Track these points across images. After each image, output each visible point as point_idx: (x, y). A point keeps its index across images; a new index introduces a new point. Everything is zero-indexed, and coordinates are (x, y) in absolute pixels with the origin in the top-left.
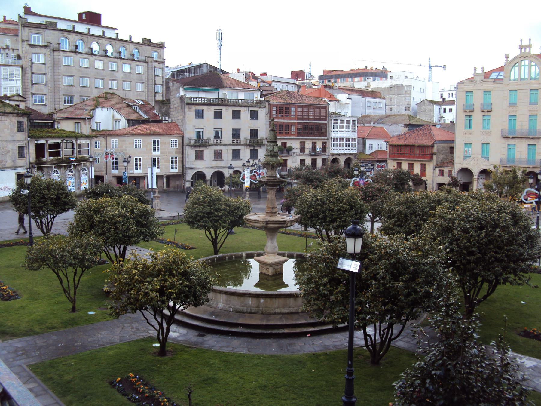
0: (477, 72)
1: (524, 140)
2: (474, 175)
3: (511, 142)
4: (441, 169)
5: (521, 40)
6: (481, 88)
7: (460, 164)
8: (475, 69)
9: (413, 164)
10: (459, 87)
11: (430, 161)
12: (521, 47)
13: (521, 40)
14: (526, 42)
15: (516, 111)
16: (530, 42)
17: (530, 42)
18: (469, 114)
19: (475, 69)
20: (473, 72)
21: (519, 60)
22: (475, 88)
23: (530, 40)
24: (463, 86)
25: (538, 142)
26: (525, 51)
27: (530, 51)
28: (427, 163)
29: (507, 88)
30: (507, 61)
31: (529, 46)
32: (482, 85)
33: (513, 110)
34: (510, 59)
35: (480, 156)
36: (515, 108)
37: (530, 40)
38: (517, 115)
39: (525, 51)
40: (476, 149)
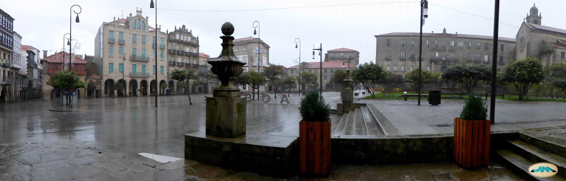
1: (140, 62)
3: (134, 63)
4: (91, 80)
5: (137, 8)
7: (107, 77)
8: (114, 18)
12: (137, 11)
13: (137, 8)
14: (139, 9)
15: (136, 46)
19: (114, 18)
22: (115, 30)
23: (141, 9)
24: (107, 27)
25: (146, 64)
29: (132, 32)
31: (141, 12)
35: (118, 71)
37: (141, 9)
38: (137, 48)
40: (116, 67)
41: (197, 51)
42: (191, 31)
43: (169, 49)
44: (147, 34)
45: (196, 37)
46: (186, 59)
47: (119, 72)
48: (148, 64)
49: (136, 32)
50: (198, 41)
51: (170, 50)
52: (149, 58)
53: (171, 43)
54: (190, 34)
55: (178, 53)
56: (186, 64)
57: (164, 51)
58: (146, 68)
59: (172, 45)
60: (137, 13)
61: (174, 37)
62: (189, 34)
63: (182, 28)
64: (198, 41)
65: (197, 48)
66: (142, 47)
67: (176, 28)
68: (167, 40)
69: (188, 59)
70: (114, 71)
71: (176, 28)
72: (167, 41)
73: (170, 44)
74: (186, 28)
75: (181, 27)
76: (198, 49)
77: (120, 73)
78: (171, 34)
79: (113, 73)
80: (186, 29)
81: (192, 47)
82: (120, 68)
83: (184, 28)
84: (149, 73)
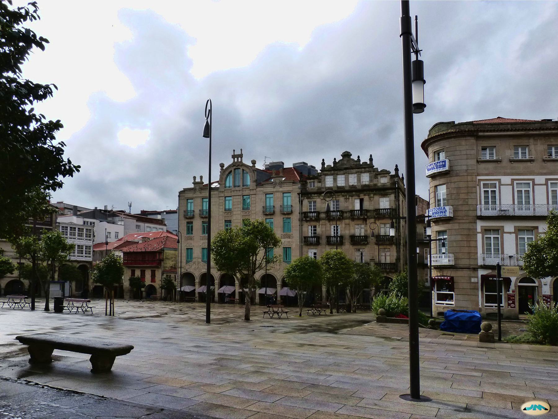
0: (196, 181)
2: (196, 278)
5: (234, 151)
6: (200, 196)
8: (195, 178)
9: (145, 271)
10: (181, 195)
11: (158, 268)
12: (234, 157)
13: (234, 151)
14: (238, 152)
15: (231, 216)
16: (241, 152)
17: (241, 152)
18: (189, 221)
19: (195, 178)
20: (193, 181)
21: (232, 169)
22: (195, 196)
23: (241, 150)
26: (238, 160)
27: (242, 160)
28: (156, 270)
29: (222, 195)
30: (222, 169)
31: (241, 156)
32: (201, 193)
33: (228, 215)
34: (224, 168)
35: (200, 260)
36: (229, 213)
37: (241, 150)
39: (238, 160)
42: (371, 160)
43: (305, 210)
44: (252, 192)
47: (202, 261)
49: (231, 192)
53: (308, 198)
54: (369, 167)
59: (315, 202)
60: (234, 160)
61: (319, 185)
63: (340, 161)
66: (243, 216)
68: (299, 194)
70: (194, 260)
74: (354, 157)
75: (339, 158)
77: (202, 263)
79: (191, 264)
80: (356, 159)
81: (372, 195)
82: (203, 256)
83: (346, 158)
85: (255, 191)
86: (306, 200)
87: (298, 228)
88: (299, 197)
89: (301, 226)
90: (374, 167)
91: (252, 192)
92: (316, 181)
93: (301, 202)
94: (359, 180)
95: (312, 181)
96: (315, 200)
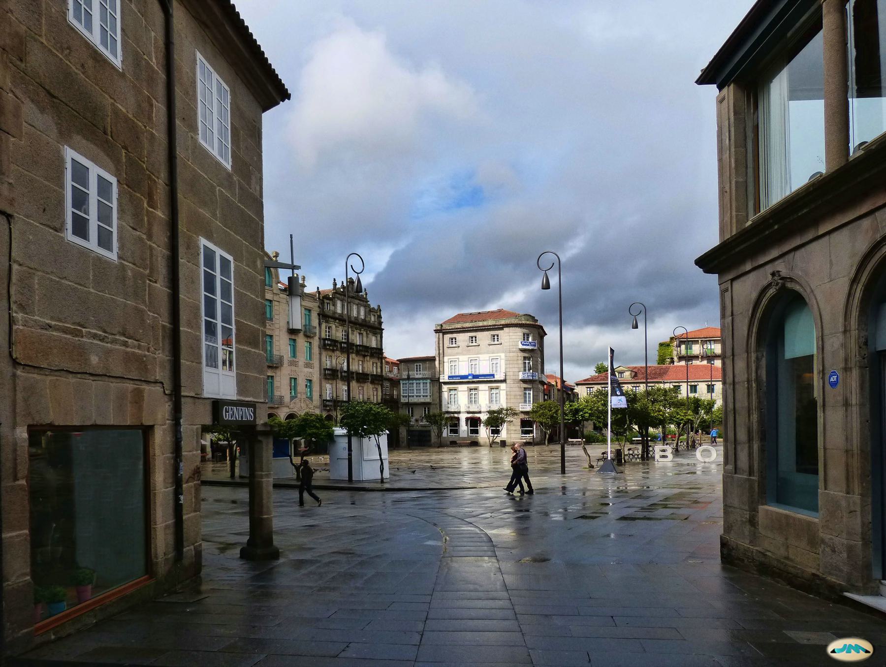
41: (379, 343)
43: (323, 336)
44: (276, 298)
45: (376, 308)
46: (357, 364)
48: (278, 373)
50: (380, 317)
51: (325, 340)
52: (281, 358)
53: (327, 322)
55: (341, 347)
56: (358, 374)
57: (311, 341)
58: (276, 384)
62: (363, 301)
64: (381, 318)
65: (379, 336)
67: (335, 284)
68: (319, 315)
69: (361, 363)
71: (335, 284)
72: (317, 317)
73: (324, 325)
76: (381, 337)
78: (326, 301)
84: (281, 397)
85: (278, 296)
86: (324, 323)
87: (318, 356)
88: (319, 319)
89: (320, 354)
90: (369, 301)
91: (276, 298)
92: (331, 302)
93: (320, 324)
94: (358, 312)
95: (328, 301)
96: (331, 325)
